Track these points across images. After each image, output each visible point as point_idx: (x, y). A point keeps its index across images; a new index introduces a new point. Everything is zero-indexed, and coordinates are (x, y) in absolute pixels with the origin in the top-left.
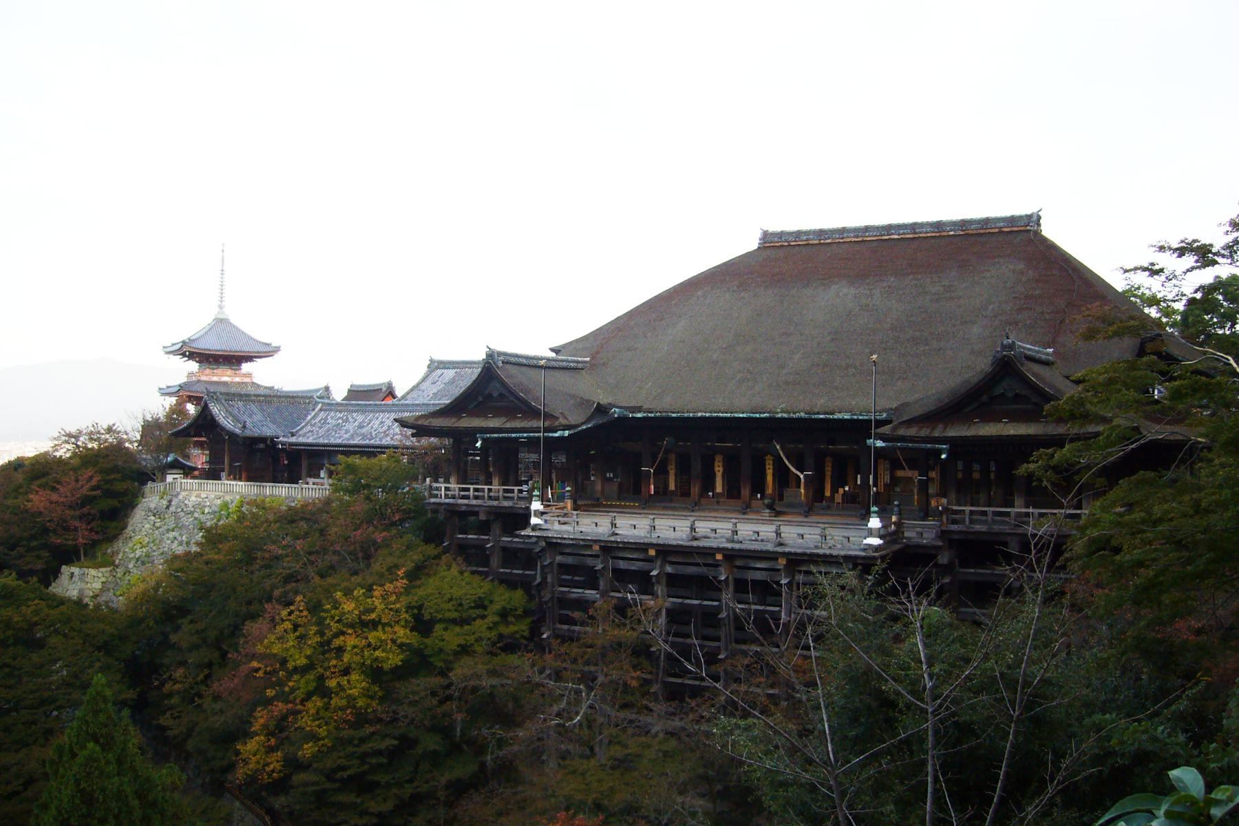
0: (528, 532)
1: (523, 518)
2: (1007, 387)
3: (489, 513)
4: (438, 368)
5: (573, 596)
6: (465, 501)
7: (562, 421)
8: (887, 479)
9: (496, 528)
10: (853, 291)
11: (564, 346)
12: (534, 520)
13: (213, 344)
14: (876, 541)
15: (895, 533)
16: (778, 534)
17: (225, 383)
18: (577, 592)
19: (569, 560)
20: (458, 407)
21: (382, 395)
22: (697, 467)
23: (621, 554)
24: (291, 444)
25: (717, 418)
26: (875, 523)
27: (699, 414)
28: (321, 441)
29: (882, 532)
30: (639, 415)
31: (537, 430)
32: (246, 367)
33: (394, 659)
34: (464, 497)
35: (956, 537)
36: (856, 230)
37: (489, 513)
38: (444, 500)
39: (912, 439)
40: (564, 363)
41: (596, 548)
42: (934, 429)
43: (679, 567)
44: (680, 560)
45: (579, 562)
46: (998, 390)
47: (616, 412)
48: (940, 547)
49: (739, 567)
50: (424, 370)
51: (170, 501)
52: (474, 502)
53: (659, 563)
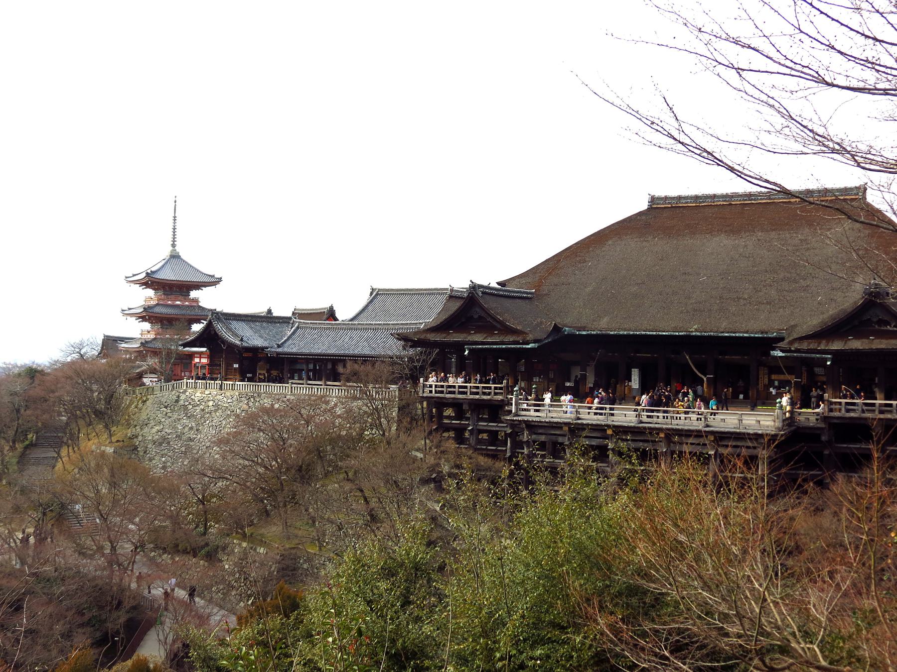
6: (452, 396)
7: (530, 337)
8: (766, 381)
13: (168, 275)
15: (790, 418)
17: (178, 306)
19: (543, 438)
20: (442, 327)
21: (325, 317)
24: (278, 354)
25: (646, 335)
28: (306, 351)
30: (584, 333)
32: (194, 294)
34: (450, 392)
35: (835, 421)
41: (566, 428)
42: (820, 343)
46: (866, 317)
48: (822, 429)
51: (178, 397)
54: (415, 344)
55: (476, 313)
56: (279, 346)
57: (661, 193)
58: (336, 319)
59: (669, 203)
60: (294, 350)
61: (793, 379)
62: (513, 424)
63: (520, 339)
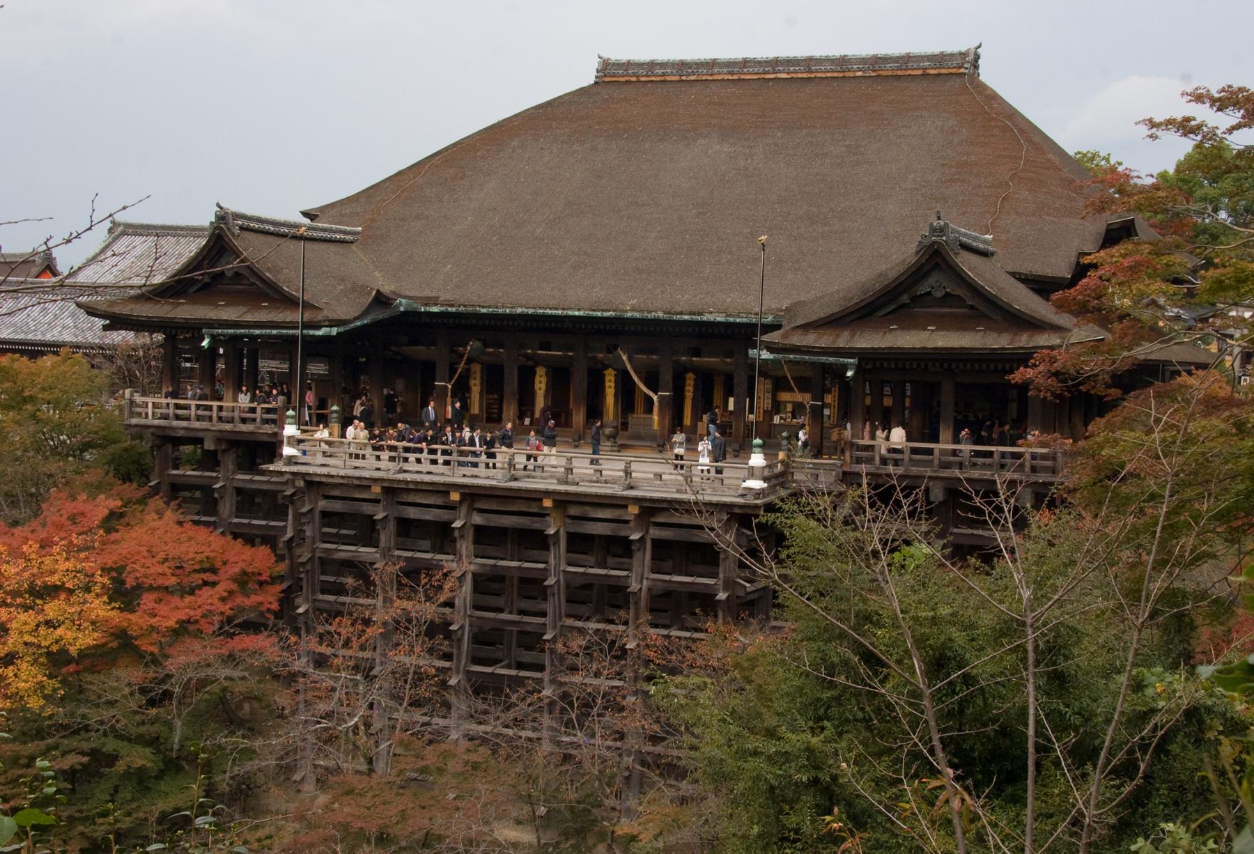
0: (277, 466)
1: (271, 448)
2: (934, 284)
3: (219, 441)
4: (123, 234)
5: (341, 555)
6: (185, 424)
8: (768, 403)
9: (229, 462)
10: (726, 148)
11: (323, 209)
12: (287, 451)
14: (757, 484)
15: (782, 474)
16: (628, 473)
18: (347, 551)
19: (338, 506)
20: (176, 288)
21: (35, 270)
22: (511, 383)
23: (412, 498)
26: (757, 460)
27: (519, 310)
29: (766, 473)
30: (435, 309)
31: (294, 326)
33: (87, 639)
36: (730, 64)
37: (219, 441)
38: (151, 421)
39: (808, 350)
40: (322, 231)
41: (377, 489)
42: (838, 336)
44: (494, 507)
45: (349, 510)
46: (923, 288)
47: (403, 304)
49: (574, 518)
52: (197, 425)
53: (464, 510)
54: (116, 322)
57: (620, 53)
59: (634, 75)
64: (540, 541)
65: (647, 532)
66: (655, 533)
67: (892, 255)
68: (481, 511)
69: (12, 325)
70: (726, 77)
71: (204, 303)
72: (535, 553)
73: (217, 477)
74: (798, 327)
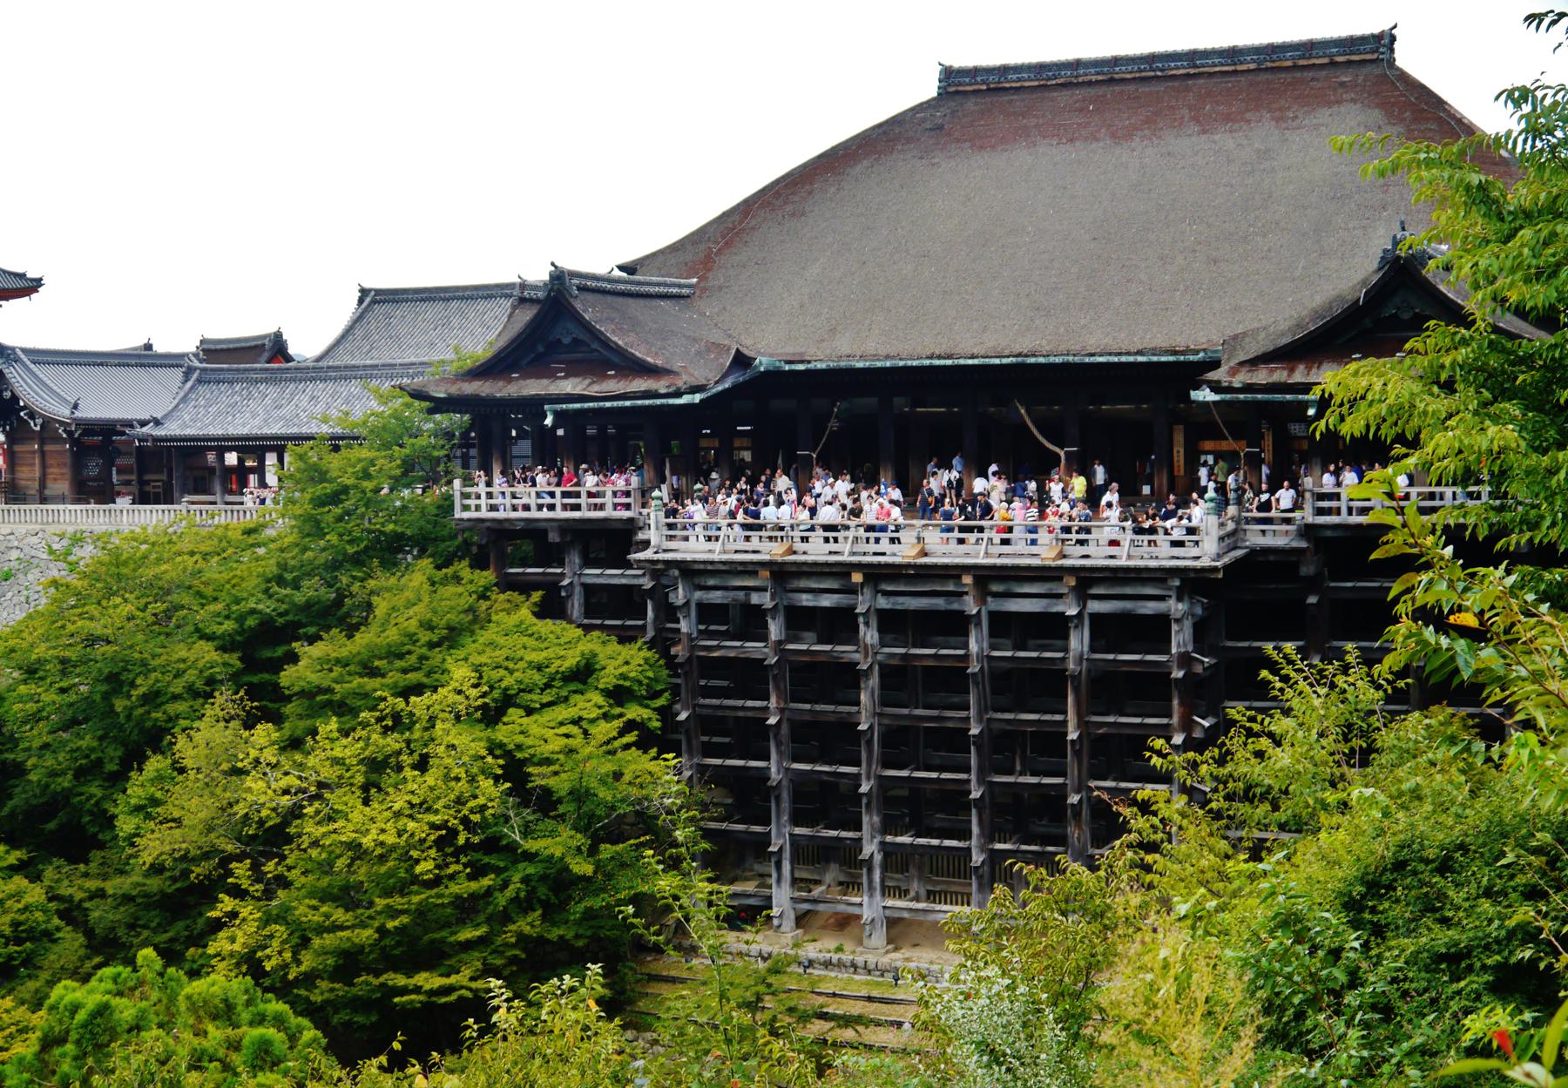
15: (1234, 533)
19: (716, 597)
21: (266, 355)
24: (156, 439)
25: (931, 367)
30: (801, 367)
42: (1292, 371)
43: (901, 599)
47: (763, 363)
50: (348, 307)
55: (566, 333)
56: (157, 422)
57: (963, 59)
58: (289, 359)
60: (189, 432)
61: (1244, 450)
62: (659, 570)
63: (661, 386)
64: (957, 625)
65: (1085, 606)
66: (1095, 606)
67: (1351, 273)
68: (887, 594)
69: (281, 418)
70: (1094, 78)
71: (539, 376)
72: (952, 640)
73: (562, 575)
74: (1242, 364)
